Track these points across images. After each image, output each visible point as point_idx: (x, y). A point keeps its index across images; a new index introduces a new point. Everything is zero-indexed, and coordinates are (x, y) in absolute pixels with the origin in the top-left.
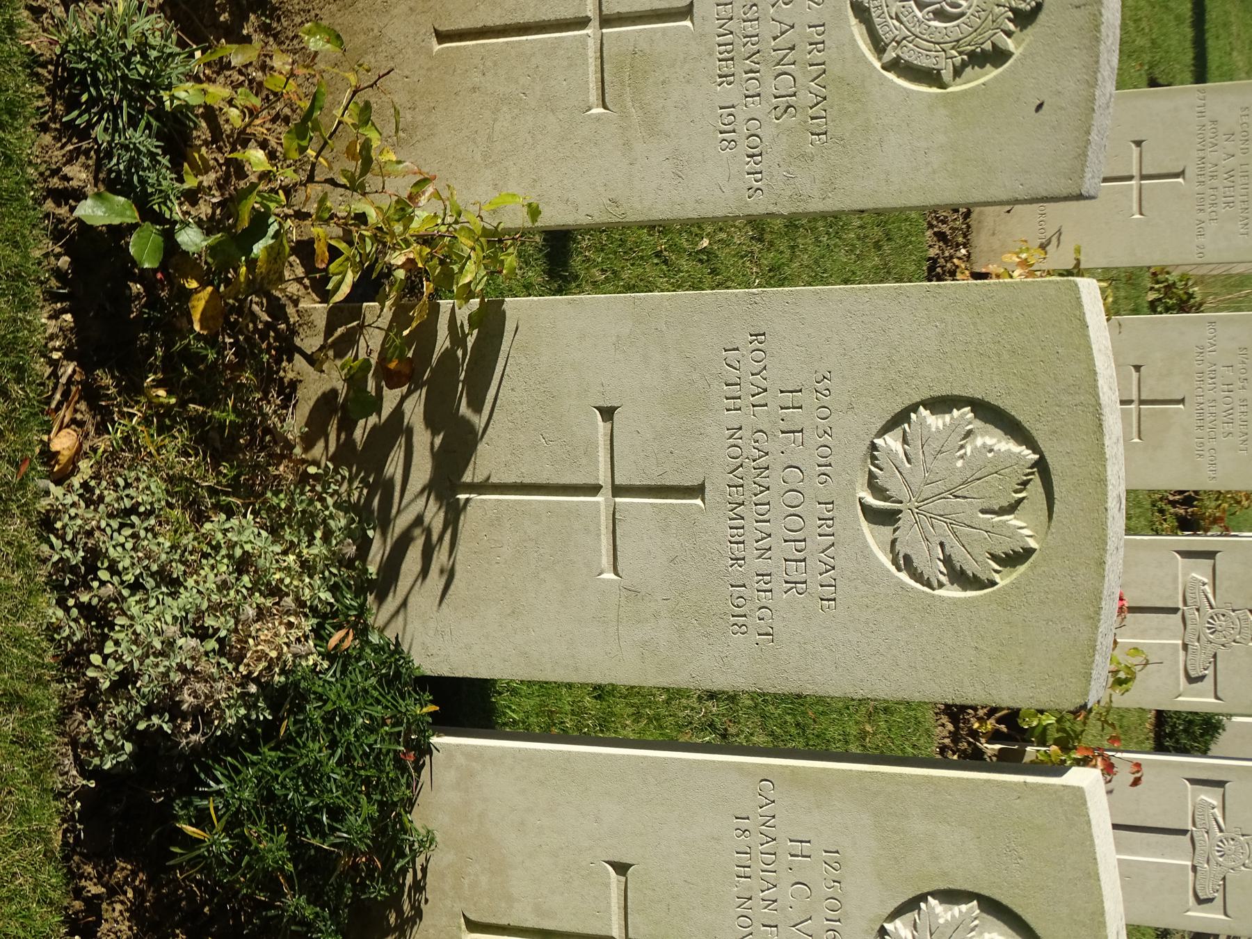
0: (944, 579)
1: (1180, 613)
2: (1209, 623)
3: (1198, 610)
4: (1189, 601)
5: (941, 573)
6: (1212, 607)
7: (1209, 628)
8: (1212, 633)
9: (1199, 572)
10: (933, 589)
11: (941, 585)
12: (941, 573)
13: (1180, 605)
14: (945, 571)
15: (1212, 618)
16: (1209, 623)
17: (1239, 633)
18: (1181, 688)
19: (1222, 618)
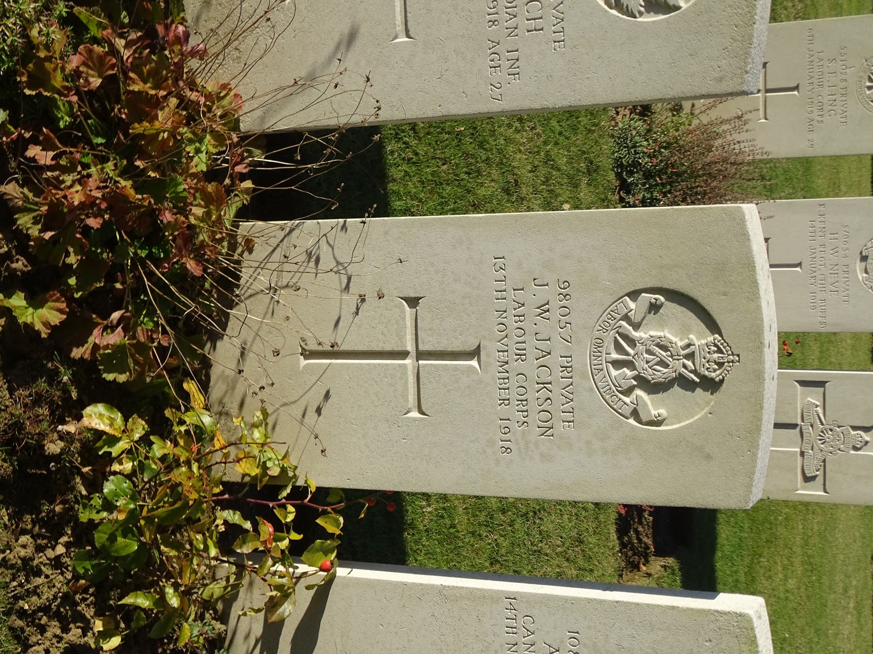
0: (642, 9)
1: (799, 427)
2: (820, 436)
3: (812, 426)
4: (805, 421)
5: (641, 6)
6: (822, 424)
7: (820, 440)
8: (822, 444)
9: (813, 397)
10: (635, 17)
11: (641, 14)
12: (641, 6)
13: (799, 422)
14: (643, 4)
15: (822, 432)
16: (820, 436)
17: (843, 444)
18: (799, 486)
19: (830, 433)
